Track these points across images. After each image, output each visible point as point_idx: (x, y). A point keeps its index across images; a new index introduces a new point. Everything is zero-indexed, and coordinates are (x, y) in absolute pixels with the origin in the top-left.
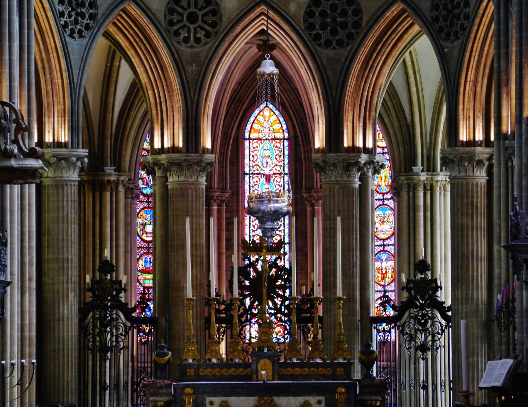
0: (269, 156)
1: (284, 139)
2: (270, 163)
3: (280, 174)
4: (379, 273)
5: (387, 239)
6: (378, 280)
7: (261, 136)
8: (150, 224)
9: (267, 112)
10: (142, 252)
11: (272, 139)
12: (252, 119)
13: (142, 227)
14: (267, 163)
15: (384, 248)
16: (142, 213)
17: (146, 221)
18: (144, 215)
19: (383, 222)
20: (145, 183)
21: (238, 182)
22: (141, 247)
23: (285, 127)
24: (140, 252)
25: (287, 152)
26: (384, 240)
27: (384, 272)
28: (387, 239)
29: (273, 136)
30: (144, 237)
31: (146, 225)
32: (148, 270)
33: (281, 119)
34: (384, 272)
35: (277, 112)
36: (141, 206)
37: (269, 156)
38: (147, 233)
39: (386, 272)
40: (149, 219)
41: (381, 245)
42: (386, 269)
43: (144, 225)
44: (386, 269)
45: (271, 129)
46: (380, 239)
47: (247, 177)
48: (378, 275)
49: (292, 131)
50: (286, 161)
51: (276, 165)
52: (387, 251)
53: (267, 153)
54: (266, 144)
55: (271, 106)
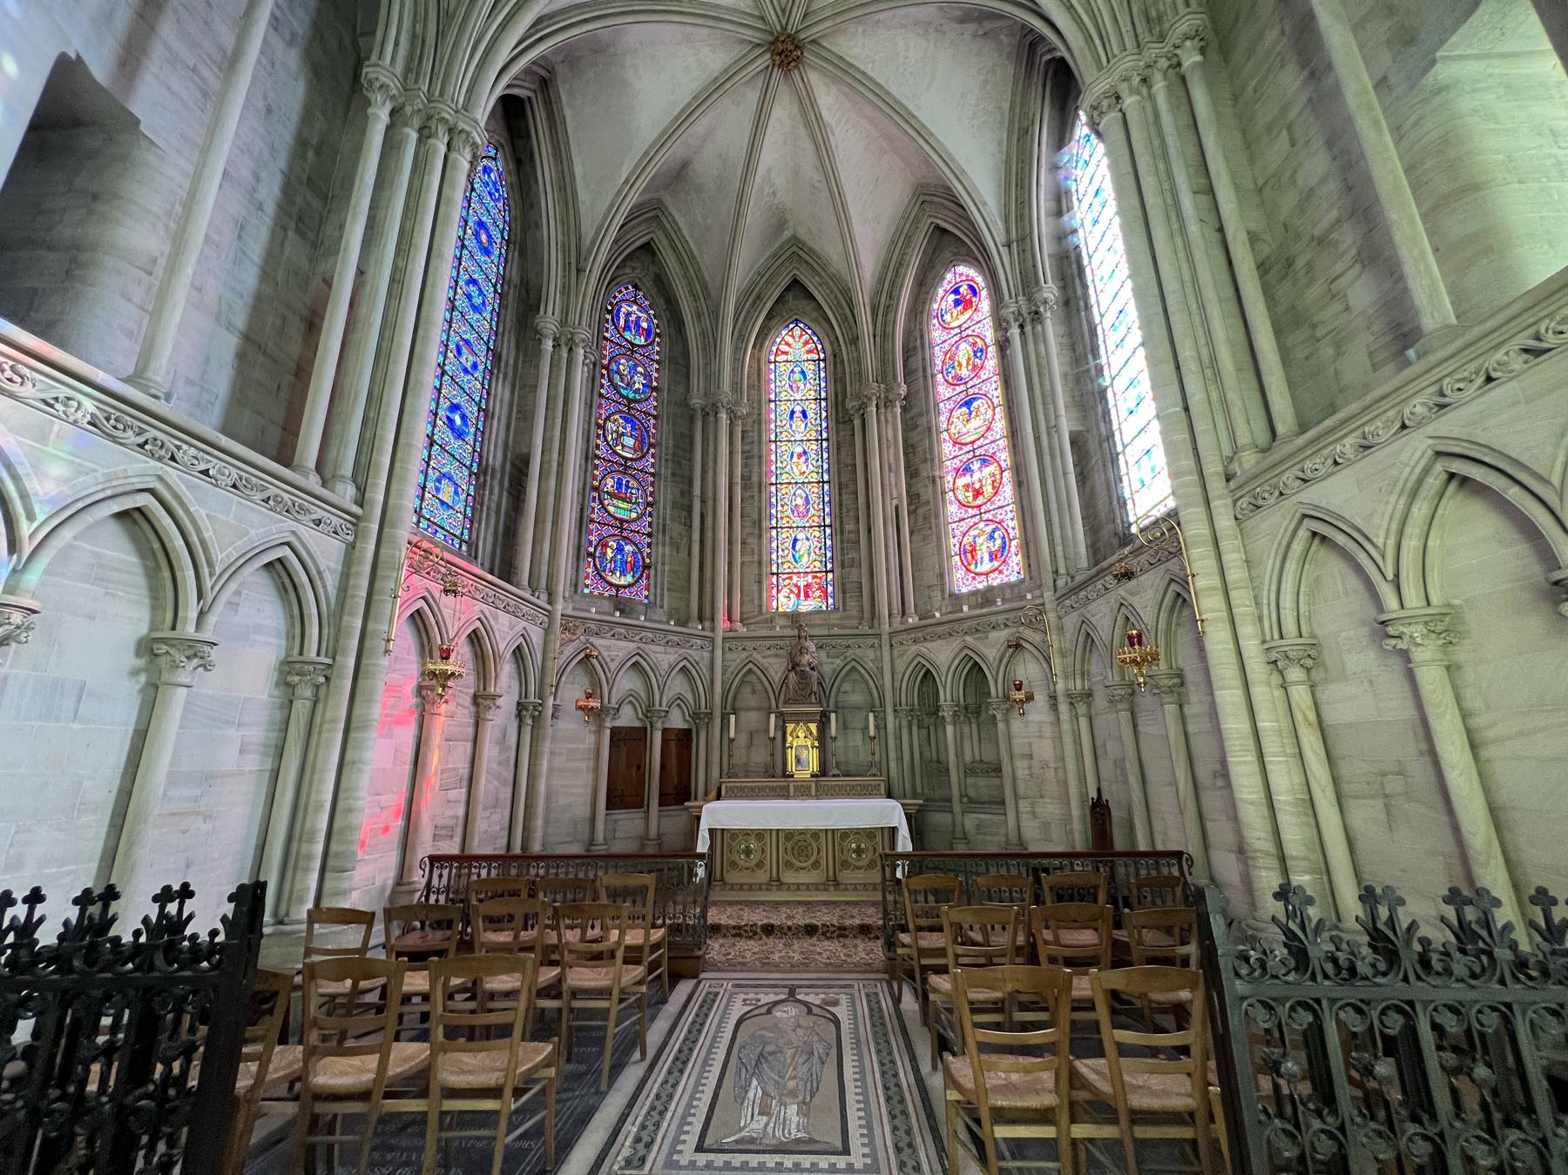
7: (790, 358)
9: (797, 332)
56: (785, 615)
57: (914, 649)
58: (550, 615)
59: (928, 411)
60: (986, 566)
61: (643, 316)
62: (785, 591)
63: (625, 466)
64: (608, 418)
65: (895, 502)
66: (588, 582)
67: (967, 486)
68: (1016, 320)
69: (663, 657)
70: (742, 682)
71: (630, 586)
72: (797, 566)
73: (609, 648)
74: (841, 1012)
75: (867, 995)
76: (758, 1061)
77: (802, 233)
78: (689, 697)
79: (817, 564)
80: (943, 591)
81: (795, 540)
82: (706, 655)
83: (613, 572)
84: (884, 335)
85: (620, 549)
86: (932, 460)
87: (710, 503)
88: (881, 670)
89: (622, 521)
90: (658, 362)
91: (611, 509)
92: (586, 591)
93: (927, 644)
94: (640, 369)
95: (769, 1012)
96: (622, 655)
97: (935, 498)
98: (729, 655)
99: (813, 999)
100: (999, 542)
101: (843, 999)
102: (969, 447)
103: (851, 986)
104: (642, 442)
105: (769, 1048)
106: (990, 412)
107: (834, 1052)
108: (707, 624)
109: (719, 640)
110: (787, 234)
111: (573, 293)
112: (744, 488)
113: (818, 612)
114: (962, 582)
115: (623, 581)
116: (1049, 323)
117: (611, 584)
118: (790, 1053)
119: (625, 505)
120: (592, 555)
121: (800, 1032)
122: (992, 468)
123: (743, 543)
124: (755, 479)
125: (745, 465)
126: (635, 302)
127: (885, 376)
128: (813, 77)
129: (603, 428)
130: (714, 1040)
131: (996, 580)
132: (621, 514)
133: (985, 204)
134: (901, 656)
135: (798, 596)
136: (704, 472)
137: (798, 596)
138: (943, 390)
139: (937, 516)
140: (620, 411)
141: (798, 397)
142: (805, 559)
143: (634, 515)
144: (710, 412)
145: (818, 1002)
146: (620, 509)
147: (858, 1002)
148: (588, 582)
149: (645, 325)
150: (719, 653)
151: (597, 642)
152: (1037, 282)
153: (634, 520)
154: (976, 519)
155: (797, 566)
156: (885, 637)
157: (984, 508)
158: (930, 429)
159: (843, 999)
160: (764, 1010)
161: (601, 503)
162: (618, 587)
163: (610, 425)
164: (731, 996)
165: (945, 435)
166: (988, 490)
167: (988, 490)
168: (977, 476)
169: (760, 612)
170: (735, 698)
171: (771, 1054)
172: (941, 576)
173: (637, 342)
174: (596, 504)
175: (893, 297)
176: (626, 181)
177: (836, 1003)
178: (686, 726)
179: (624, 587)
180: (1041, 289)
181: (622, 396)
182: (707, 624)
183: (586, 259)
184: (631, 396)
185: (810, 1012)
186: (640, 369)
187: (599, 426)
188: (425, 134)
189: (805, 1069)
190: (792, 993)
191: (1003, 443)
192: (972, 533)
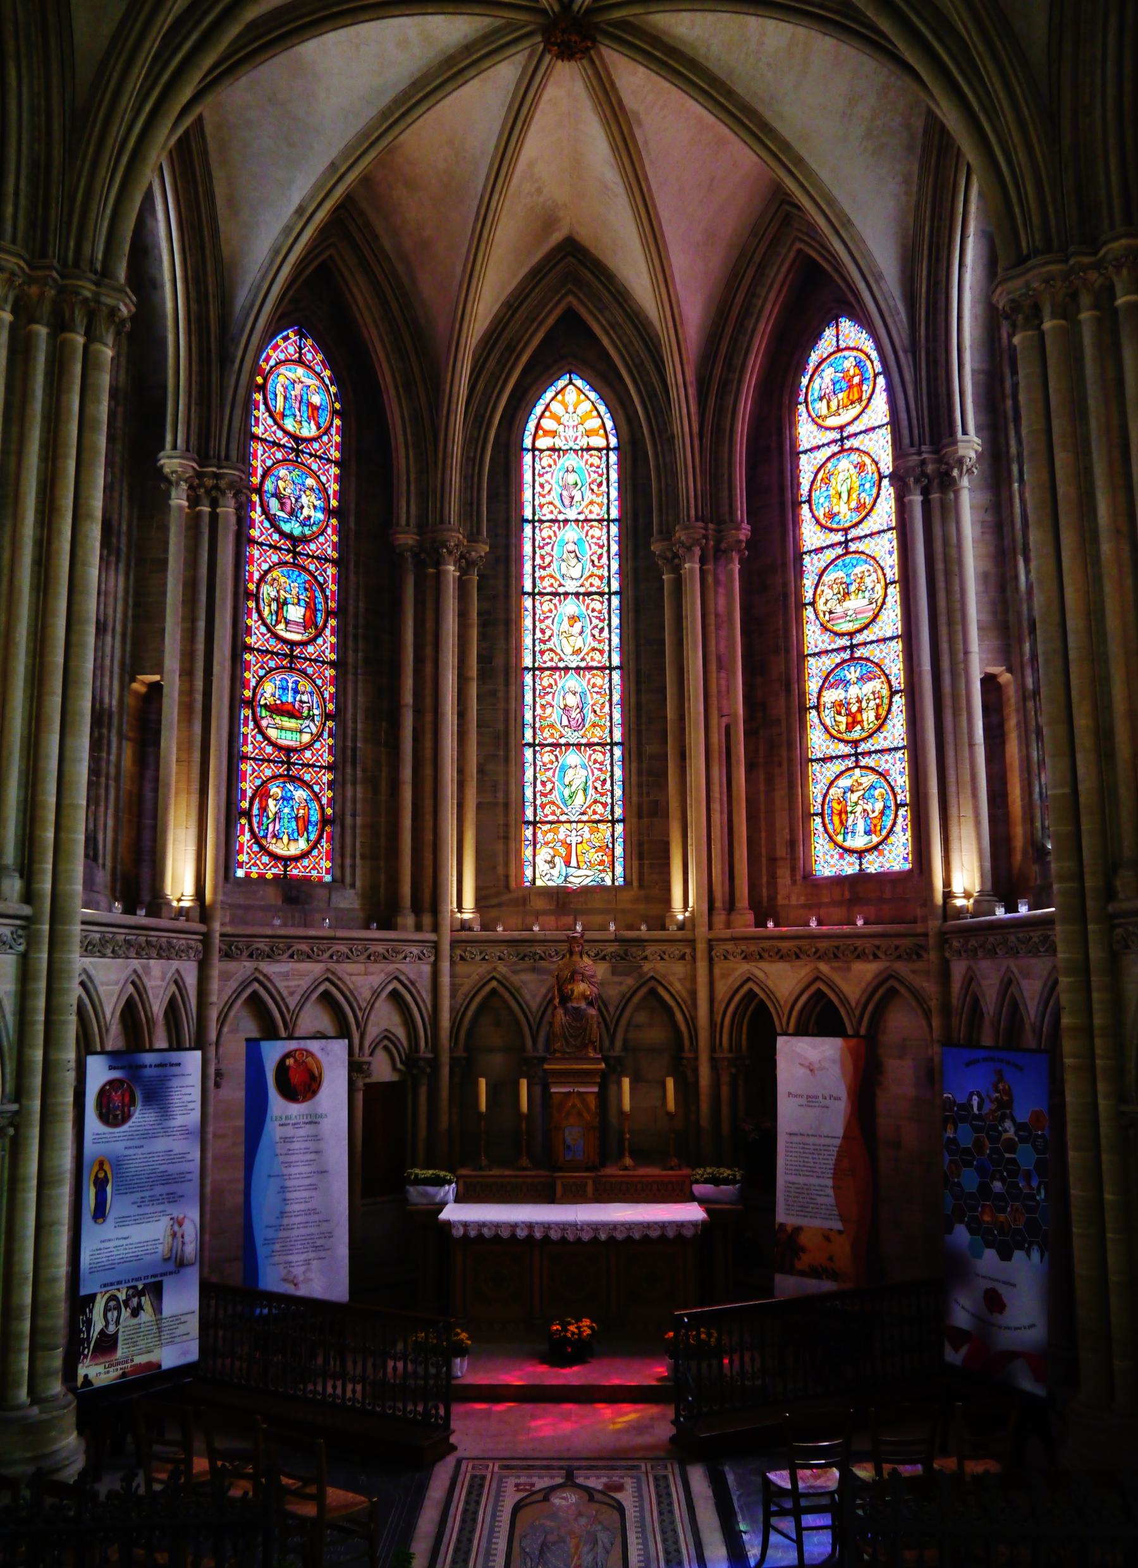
0: (576, 484)
1: (608, 448)
2: (578, 497)
3: (600, 521)
4: (839, 713)
5: (860, 631)
6: (839, 732)
7: (559, 443)
8: (298, 604)
10: (272, 664)
11: (582, 449)
12: (538, 410)
13: (274, 606)
14: (572, 498)
15: (852, 653)
16: (275, 574)
17: (288, 596)
18: (282, 580)
19: (847, 594)
20: (288, 509)
21: (508, 536)
22: (272, 653)
23: (609, 424)
25: (614, 476)
26: (851, 635)
27: (854, 709)
28: (860, 631)
29: (583, 442)
30: (280, 629)
31: (285, 603)
32: (290, 707)
33: (602, 409)
34: (854, 709)
35: (593, 395)
36: (275, 558)
37: (576, 484)
38: (287, 622)
39: (860, 710)
40: (294, 592)
41: (844, 649)
42: (859, 701)
43: (282, 604)
44: (859, 701)
45: (581, 428)
46: (841, 635)
47: (528, 528)
48: (838, 718)
49: (624, 428)
50: (614, 494)
51: (591, 503)
52: (860, 658)
53: (571, 478)
54: (571, 460)
55: (579, 382)
56: (547, 892)
57: (744, 968)
58: (206, 939)
59: (784, 565)
60: (859, 841)
61: (313, 382)
62: (544, 854)
63: (290, 658)
64: (262, 579)
65: (724, 720)
66: (243, 858)
67: (840, 707)
68: (917, 481)
69: (363, 979)
70: (482, 1007)
71: (305, 855)
72: (571, 824)
73: (286, 976)
74: (626, 1498)
75: (656, 1479)
76: (542, 1552)
77: (585, 236)
78: (401, 1033)
79: (599, 808)
80: (793, 870)
81: (564, 770)
82: (427, 969)
84: (718, 430)
86: (787, 651)
87: (429, 718)
88: (693, 994)
89: (288, 750)
90: (337, 463)
91: (272, 733)
92: (240, 873)
93: (764, 965)
95: (546, 1499)
96: (305, 983)
97: (788, 715)
98: (461, 968)
99: (596, 1482)
100: (879, 806)
101: (629, 1483)
102: (844, 642)
103: (637, 1468)
104: (315, 611)
105: (551, 1538)
106: (879, 588)
107: (619, 1539)
108: (427, 920)
109: (446, 947)
110: (557, 237)
111: (215, 402)
112: (483, 676)
113: (600, 888)
114: (827, 863)
115: (294, 850)
116: (966, 498)
117: (274, 856)
118: (574, 1542)
120: (247, 814)
121: (583, 1521)
122: (876, 685)
123: (481, 771)
124: (499, 661)
125: (482, 637)
126: (300, 362)
127: (715, 512)
128: (605, 51)
129: (256, 597)
130: (492, 1531)
131: (873, 865)
132: (288, 739)
133: (879, 277)
134: (724, 976)
135: (568, 864)
136: (419, 660)
137: (568, 864)
138: (811, 536)
139: (790, 746)
140: (282, 563)
141: (572, 514)
142: (580, 799)
143: (306, 738)
144: (429, 556)
145: (600, 1487)
147: (645, 1487)
148: (243, 858)
149: (316, 400)
150: (445, 966)
151: (271, 968)
152: (952, 433)
153: (309, 746)
154: (850, 763)
155: (571, 824)
156: (701, 947)
157: (863, 747)
158: (786, 596)
159: (629, 1483)
160: (540, 1496)
161: (257, 725)
162: (286, 860)
163: (268, 591)
164: (500, 1481)
165: (809, 612)
166: (869, 716)
167: (869, 716)
168: (854, 691)
169: (507, 887)
170: (470, 1033)
171: (554, 1543)
172: (792, 844)
174: (249, 729)
175: (733, 368)
176: (300, 211)
177: (620, 1488)
178: (394, 1077)
179: (296, 859)
180: (955, 442)
181: (283, 534)
182: (427, 920)
183: (235, 341)
184: (297, 531)
185: (591, 1499)
186: (310, 482)
187: (249, 595)
188: (60, 326)
189: (590, 1558)
190: (570, 1476)
191: (897, 646)
192: (845, 782)
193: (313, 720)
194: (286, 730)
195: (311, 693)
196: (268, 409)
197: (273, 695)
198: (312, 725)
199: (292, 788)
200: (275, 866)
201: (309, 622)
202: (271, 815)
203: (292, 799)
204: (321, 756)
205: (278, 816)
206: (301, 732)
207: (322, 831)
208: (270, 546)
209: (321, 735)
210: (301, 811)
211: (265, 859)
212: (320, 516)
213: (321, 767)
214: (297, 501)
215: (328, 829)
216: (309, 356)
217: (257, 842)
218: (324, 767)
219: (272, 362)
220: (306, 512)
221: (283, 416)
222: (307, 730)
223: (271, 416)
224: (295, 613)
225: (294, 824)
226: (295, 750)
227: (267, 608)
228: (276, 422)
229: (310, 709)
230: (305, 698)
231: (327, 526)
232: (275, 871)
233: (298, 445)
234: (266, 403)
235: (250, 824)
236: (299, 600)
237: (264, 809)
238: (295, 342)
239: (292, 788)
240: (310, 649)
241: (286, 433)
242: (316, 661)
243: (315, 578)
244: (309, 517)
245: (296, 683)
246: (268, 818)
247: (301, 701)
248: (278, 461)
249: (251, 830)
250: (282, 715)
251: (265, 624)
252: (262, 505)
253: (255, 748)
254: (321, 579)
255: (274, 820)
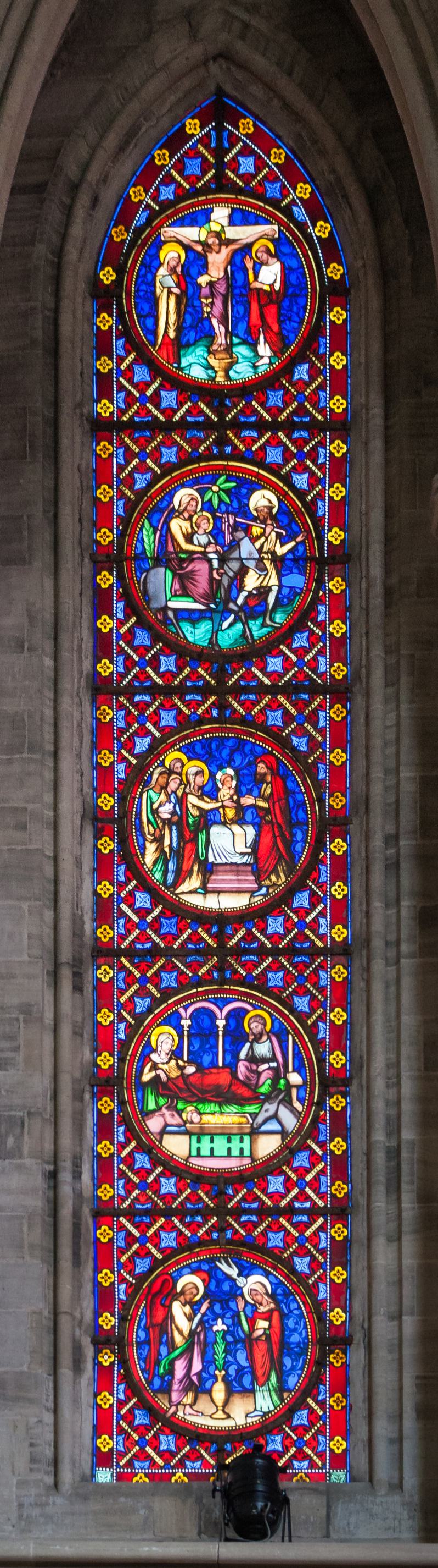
8: (240, 820)
13: (170, 839)
16: (172, 757)
17: (208, 805)
18: (193, 767)
20: (202, 584)
24: (156, 980)
30: (190, 893)
31: (206, 820)
32: (224, 1078)
38: (208, 869)
40: (226, 792)
43: (191, 830)
83: (199, 1387)
85: (221, 1296)
91: (176, 1146)
94: (261, 499)
119: (230, 1117)
132: (220, 1156)
143: (268, 1145)
146: (211, 1139)
153: (273, 1165)
173: (243, 372)
193: (288, 1102)
194: (212, 1134)
195: (280, 1034)
196: (132, 344)
197: (176, 1054)
198: (284, 1113)
199: (233, 1272)
200: (197, 1457)
201: (259, 863)
202: (178, 1339)
203: (236, 1292)
204: (315, 1184)
205: (200, 1339)
206: (255, 1132)
207: (321, 1363)
208: (154, 690)
209: (313, 1133)
210: (262, 1324)
211: (167, 1442)
212: (296, 580)
213: (314, 1213)
214: (223, 560)
215: (335, 1360)
216: (247, 165)
217: (143, 1404)
218: (323, 1212)
219: (140, 218)
220: (252, 581)
221: (179, 345)
222: (273, 1126)
223: (144, 358)
224: (230, 843)
225: (242, 1357)
226: (239, 1178)
227: (151, 848)
228: (156, 370)
229: (277, 1075)
230: (263, 1049)
231: (317, 601)
232: (194, 1467)
233: (221, 410)
234: (126, 332)
235: (123, 1361)
236: (240, 809)
237: (163, 1326)
238: (205, 141)
239: (233, 1272)
240: (275, 925)
241: (187, 388)
242: (290, 951)
243: (285, 744)
244: (263, 591)
245: (237, 1015)
246: (172, 1346)
247: (253, 1059)
248: (167, 469)
249: (127, 1378)
250: (203, 1101)
251: (145, 885)
252: (126, 596)
253: (129, 1186)
254: (300, 743)
255: (189, 1350)
